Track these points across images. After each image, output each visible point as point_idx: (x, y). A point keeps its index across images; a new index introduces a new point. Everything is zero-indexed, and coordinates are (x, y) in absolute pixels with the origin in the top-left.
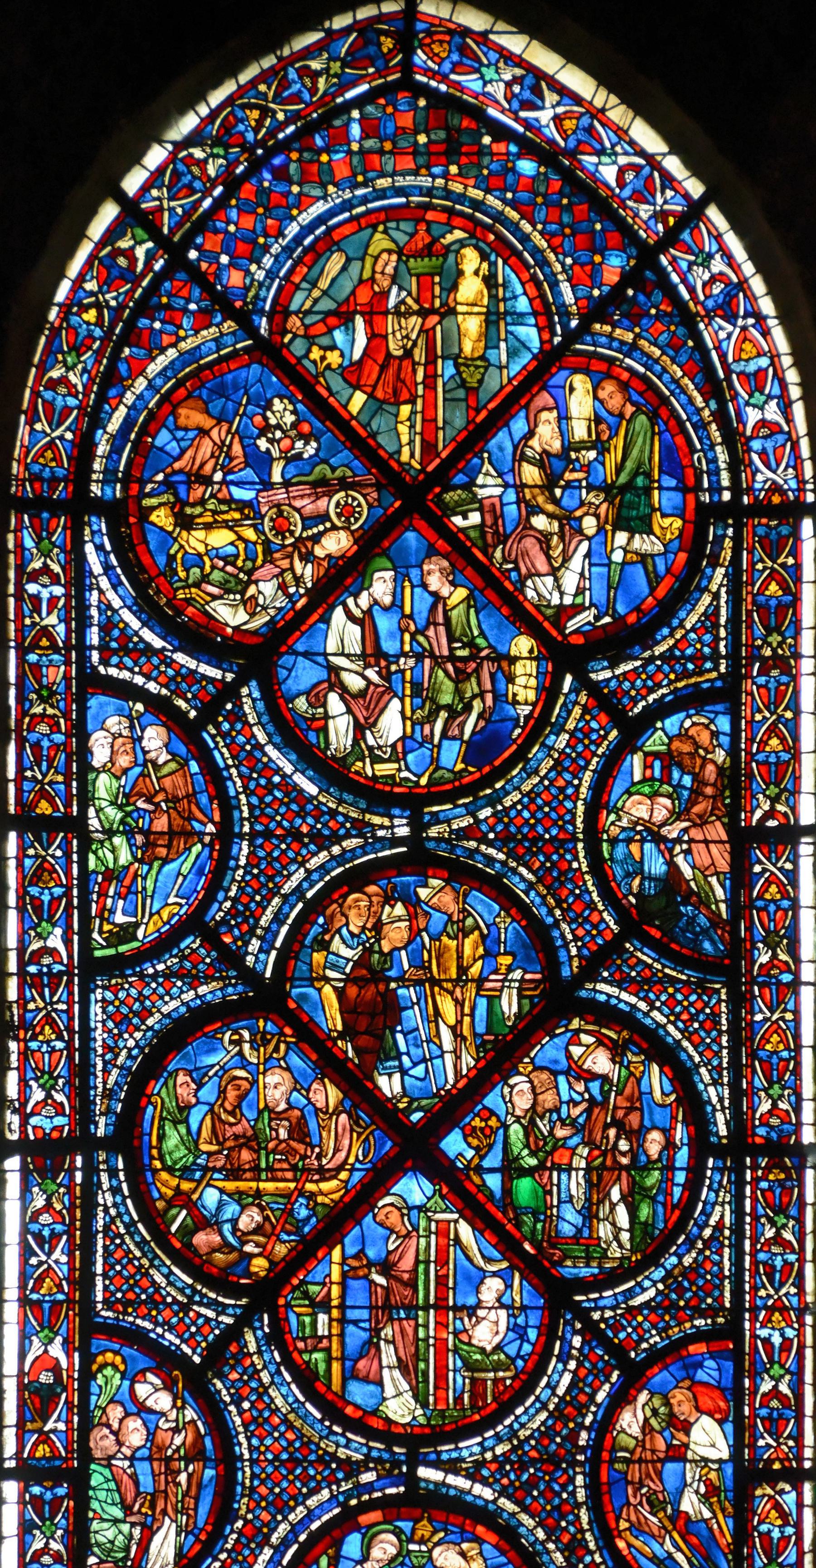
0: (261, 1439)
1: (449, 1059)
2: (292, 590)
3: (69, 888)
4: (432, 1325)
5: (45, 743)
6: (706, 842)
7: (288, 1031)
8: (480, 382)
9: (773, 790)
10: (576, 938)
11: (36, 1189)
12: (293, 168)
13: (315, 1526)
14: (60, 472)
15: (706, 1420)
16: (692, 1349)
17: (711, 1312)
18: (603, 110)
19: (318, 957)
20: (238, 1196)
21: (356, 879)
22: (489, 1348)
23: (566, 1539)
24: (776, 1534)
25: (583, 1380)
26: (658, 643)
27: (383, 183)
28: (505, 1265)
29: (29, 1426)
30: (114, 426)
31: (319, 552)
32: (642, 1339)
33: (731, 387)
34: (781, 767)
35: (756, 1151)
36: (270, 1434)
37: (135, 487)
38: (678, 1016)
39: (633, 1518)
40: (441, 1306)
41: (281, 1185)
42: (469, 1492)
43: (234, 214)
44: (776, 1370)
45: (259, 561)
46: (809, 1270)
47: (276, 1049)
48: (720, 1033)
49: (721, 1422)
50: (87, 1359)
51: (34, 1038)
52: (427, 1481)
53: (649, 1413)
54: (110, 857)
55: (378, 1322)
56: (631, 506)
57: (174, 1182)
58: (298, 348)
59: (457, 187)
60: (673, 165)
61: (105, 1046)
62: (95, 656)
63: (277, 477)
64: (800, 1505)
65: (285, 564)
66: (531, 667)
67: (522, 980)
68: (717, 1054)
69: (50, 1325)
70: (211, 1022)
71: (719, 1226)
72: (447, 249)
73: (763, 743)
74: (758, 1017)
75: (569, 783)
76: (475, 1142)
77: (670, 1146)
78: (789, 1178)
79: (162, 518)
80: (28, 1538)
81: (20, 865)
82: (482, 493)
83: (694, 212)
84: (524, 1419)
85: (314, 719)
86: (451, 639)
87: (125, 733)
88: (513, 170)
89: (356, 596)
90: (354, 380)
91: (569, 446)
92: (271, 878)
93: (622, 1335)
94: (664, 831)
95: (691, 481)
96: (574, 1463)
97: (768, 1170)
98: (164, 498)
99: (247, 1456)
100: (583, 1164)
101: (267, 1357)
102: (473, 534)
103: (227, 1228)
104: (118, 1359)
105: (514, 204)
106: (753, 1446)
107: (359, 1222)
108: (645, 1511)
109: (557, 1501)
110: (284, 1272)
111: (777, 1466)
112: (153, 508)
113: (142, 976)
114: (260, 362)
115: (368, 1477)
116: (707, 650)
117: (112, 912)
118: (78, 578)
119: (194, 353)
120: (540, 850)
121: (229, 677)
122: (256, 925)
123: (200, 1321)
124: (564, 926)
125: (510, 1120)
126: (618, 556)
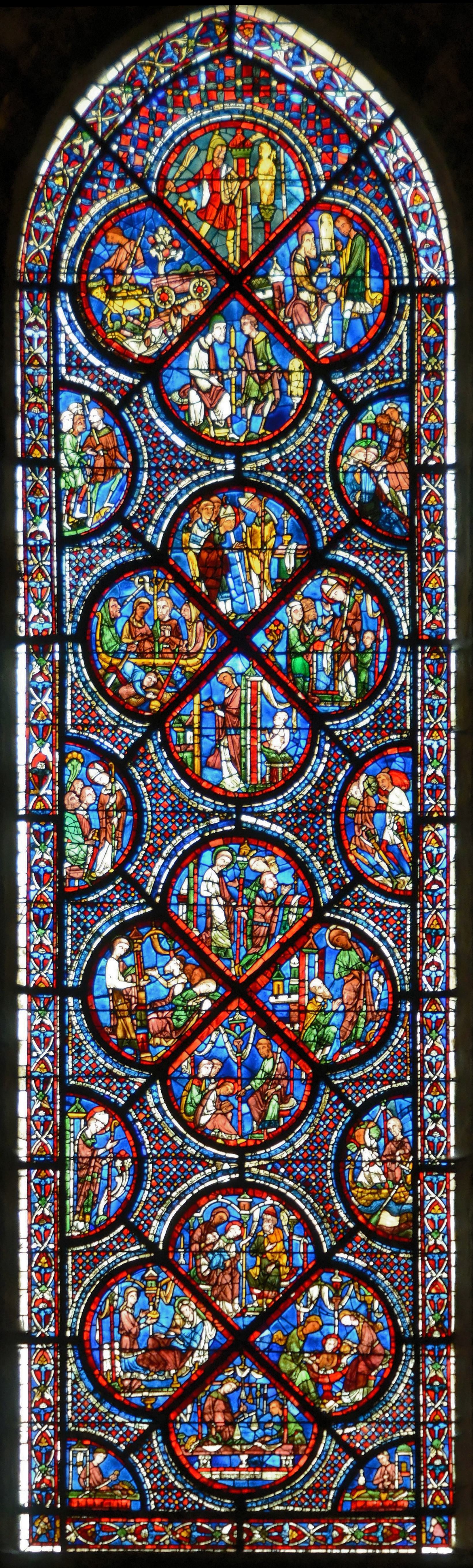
0: (157, 800)
1: (257, 593)
2: (170, 334)
3: (50, 497)
4: (249, 738)
5: (37, 418)
6: (396, 473)
7: (170, 577)
8: (272, 218)
9: (432, 444)
10: (325, 526)
11: (34, 663)
12: (169, 99)
13: (186, 847)
14: (44, 268)
15: (397, 790)
16: (389, 751)
17: (400, 731)
18: (338, 67)
19: (185, 536)
20: (144, 667)
21: (206, 493)
22: (279, 751)
23: (322, 854)
24: (435, 852)
26: (369, 363)
27: (218, 107)
28: (288, 705)
29: (32, 792)
30: (73, 242)
31: (185, 312)
32: (362, 746)
33: (408, 221)
34: (437, 431)
35: (424, 643)
37: (84, 276)
38: (381, 569)
40: (253, 728)
41: (167, 661)
43: (137, 125)
44: (435, 763)
45: (152, 317)
46: (453, 708)
47: (163, 587)
48: (404, 578)
49: (405, 791)
50: (63, 756)
51: (33, 579)
54: (72, 480)
56: (355, 286)
57: (109, 659)
58: (172, 199)
59: (258, 110)
60: (377, 97)
61: (71, 585)
62: (63, 370)
63: (161, 271)
64: (448, 836)
65: (166, 319)
66: (301, 376)
67: (296, 549)
68: (403, 590)
69: (42, 737)
70: (129, 571)
71: (404, 684)
72: (253, 144)
73: (427, 418)
74: (425, 570)
75: (321, 440)
76: (272, 638)
77: (377, 640)
78: (442, 658)
79: (99, 293)
81: (24, 486)
82: (273, 280)
83: (388, 123)
84: (299, 789)
85: (182, 405)
86: (257, 360)
87: (80, 412)
88: (289, 100)
89: (205, 336)
90: (203, 217)
91: (320, 254)
92: (160, 493)
93: (352, 744)
94: (374, 467)
95: (387, 273)
96: (325, 814)
97: (430, 653)
98: (100, 283)
99: (149, 809)
100: (330, 650)
101: (160, 755)
102: (268, 303)
103: (138, 685)
104: (80, 756)
105: (290, 119)
106: (422, 804)
107: (209, 681)
110: (168, 709)
111: (435, 815)
112: (93, 288)
113: (90, 547)
114: (151, 207)
115: (215, 821)
116: (396, 367)
117: (73, 511)
118: (54, 327)
119: (115, 203)
120: (306, 477)
121: (137, 381)
122: (152, 518)
124: (319, 519)
125: (290, 626)
126: (347, 315)
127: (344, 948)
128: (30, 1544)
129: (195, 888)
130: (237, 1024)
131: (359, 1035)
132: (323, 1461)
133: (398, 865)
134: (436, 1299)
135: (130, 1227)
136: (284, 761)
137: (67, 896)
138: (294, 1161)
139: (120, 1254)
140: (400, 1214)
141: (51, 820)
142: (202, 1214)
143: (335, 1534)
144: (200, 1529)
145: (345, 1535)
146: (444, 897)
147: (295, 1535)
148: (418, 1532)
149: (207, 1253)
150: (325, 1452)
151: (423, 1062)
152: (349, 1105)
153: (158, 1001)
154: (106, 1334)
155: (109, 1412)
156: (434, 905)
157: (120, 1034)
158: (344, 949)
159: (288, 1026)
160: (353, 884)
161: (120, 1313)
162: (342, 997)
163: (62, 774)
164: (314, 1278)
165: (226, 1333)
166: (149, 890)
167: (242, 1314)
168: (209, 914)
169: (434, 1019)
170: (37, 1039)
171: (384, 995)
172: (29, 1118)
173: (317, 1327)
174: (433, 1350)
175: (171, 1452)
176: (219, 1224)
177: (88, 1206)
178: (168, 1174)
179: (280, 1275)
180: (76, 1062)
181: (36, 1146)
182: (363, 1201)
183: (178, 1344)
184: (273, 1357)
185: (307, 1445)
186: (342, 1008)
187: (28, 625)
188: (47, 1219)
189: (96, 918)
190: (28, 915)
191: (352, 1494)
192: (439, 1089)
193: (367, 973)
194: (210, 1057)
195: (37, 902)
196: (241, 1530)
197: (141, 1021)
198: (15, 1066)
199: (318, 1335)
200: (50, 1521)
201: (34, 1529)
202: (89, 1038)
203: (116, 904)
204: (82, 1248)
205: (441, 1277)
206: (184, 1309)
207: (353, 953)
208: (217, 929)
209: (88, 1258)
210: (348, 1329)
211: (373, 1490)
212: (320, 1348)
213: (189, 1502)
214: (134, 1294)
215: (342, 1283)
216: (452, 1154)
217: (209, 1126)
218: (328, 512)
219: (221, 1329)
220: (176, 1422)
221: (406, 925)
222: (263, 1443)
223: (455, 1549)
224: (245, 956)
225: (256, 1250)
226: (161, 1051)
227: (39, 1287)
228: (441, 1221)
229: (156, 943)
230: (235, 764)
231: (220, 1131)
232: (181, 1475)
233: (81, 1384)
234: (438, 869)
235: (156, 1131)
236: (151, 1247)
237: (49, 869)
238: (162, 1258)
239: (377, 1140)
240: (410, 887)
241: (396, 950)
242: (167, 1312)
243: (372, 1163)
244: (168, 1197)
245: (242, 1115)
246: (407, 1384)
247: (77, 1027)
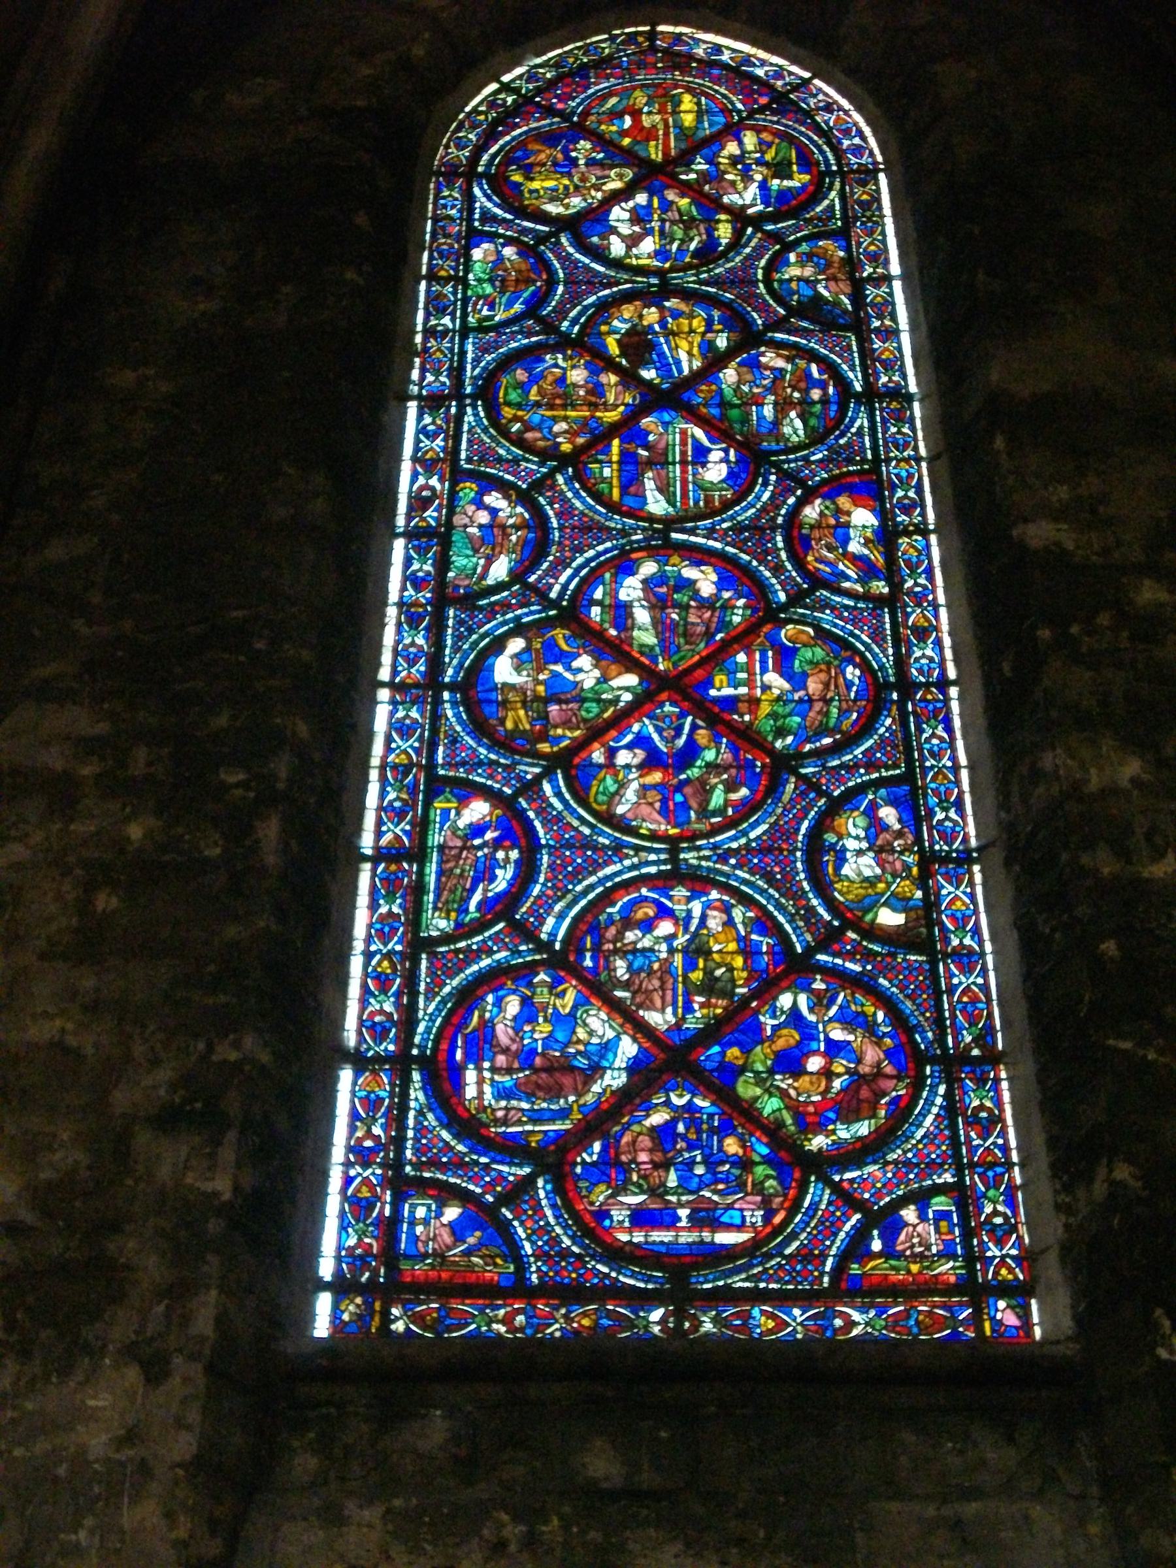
71: (861, 428)
106: (894, 519)
108: (825, 552)
132: (812, 1217)
140: (905, 910)
141: (436, 540)
143: (838, 1322)
144: (609, 1314)
145: (856, 1324)
147: (771, 1324)
150: (814, 1206)
151: (921, 750)
157: (509, 725)
158: (805, 645)
182: (851, 897)
185: (785, 1195)
187: (421, 388)
198: (368, 755)
200: (364, 1302)
213: (596, 1276)
218: (763, 308)
222: (715, 1192)
225: (697, 950)
227: (375, 997)
235: (553, 820)
243: (860, 853)
244: (569, 891)
246: (938, 1115)
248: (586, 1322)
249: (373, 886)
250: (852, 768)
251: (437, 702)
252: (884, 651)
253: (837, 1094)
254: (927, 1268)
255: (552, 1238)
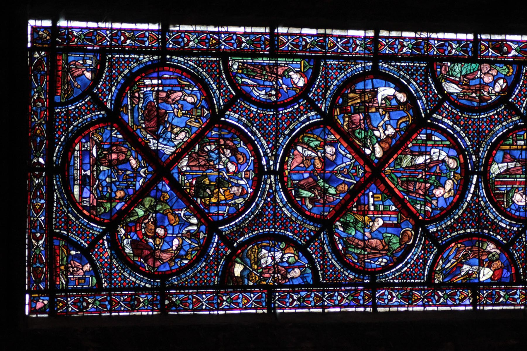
0: (486, 122)
4: (520, 180)
16: (513, 268)
22: (513, 199)
24: (457, 297)
25: (504, 231)
29: (491, 43)
36: (487, 125)
39: (461, 248)
42: (469, 192)
44: (507, 297)
49: (491, 278)
52: (473, 178)
53: (493, 253)
55: (521, 161)
64: (466, 305)
69: (520, 51)
80: (456, 42)
84: (492, 211)
93: (517, 244)
96: (478, 228)
99: (481, 117)
101: (511, 124)
104: (511, 74)
106: (484, 289)
109: (466, 222)
111: (478, 297)
115: (474, 158)
123: (522, 102)
127: (401, 240)
128: (32, 27)
129: (435, 145)
130: (356, 171)
131: (350, 249)
132: (86, 226)
133: (449, 274)
134: (189, 301)
135: (234, 99)
136: (508, 202)
137: (431, 63)
138: (275, 207)
139: (218, 92)
141: (473, 55)
142: (243, 147)
143: (38, 235)
144: (42, 142)
146: (430, 303)
147: (37, 207)
148: (39, 291)
149: (218, 149)
150: (92, 228)
151: (334, 291)
152: (308, 243)
153: (370, 120)
154: (168, 82)
155: (118, 83)
156: (425, 297)
157: (351, 95)
159: (355, 204)
160: (438, 246)
161: (181, 91)
162: (372, 238)
163: (500, 62)
164: (202, 220)
165: (169, 161)
166: (435, 115)
167: (180, 172)
168: (421, 154)
169: (360, 298)
170: (348, 42)
171: (374, 266)
172: (301, 35)
173: (172, 222)
174: (157, 300)
175: (92, 123)
176: (236, 158)
177: (247, 71)
178: (267, 124)
179: (204, 197)
180: (334, 66)
181: (284, 39)
183: (161, 129)
184: (153, 193)
185: (97, 216)
186: (366, 238)
188: (239, 45)
189: (418, 81)
190: (421, 38)
191: (64, 246)
192: (318, 301)
193: (387, 255)
194: (337, 153)
195: (428, 45)
196: (41, 170)
197: (358, 109)
198: (333, 28)
199: (167, 223)
201: (42, 30)
202: (348, 75)
203: (427, 94)
204: (221, 67)
205: (203, 304)
206: (183, 133)
207: (398, 245)
208: (412, 158)
209: (215, 71)
210: (170, 243)
211: (67, 261)
212: (158, 224)
213: (59, 136)
214: (193, 101)
215: (199, 239)
216: (279, 311)
217: (296, 152)
219: (170, 158)
220: (111, 128)
221: (415, 280)
222: (98, 186)
223: (28, 316)
224: (396, 176)
225: (220, 182)
226: (340, 122)
227: (197, 38)
228: (237, 304)
229: (404, 120)
230: (506, 171)
231: (293, 159)
232: (77, 130)
233: (136, 64)
234: (447, 299)
235: (293, 117)
236: (222, 113)
237: (446, 53)
238: (216, 120)
239: (287, 262)
240: (436, 281)
241: (400, 273)
242: (182, 123)
243: (273, 258)
244: (253, 124)
245: (302, 173)
246: (135, 283)
247: (355, 68)
248: (38, 131)
249: (258, 33)
250: (324, 256)
251: (366, 60)
252: (396, 278)
253: (146, 240)
254: (63, 273)
255: (77, 118)
